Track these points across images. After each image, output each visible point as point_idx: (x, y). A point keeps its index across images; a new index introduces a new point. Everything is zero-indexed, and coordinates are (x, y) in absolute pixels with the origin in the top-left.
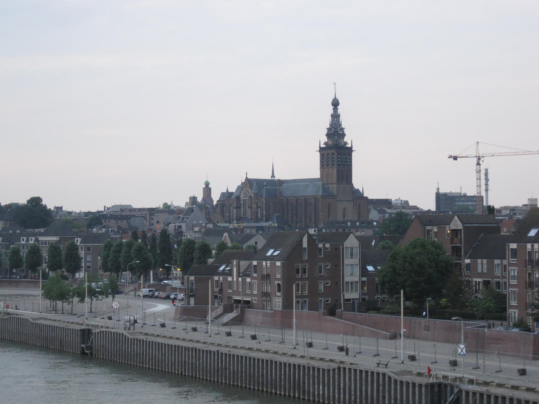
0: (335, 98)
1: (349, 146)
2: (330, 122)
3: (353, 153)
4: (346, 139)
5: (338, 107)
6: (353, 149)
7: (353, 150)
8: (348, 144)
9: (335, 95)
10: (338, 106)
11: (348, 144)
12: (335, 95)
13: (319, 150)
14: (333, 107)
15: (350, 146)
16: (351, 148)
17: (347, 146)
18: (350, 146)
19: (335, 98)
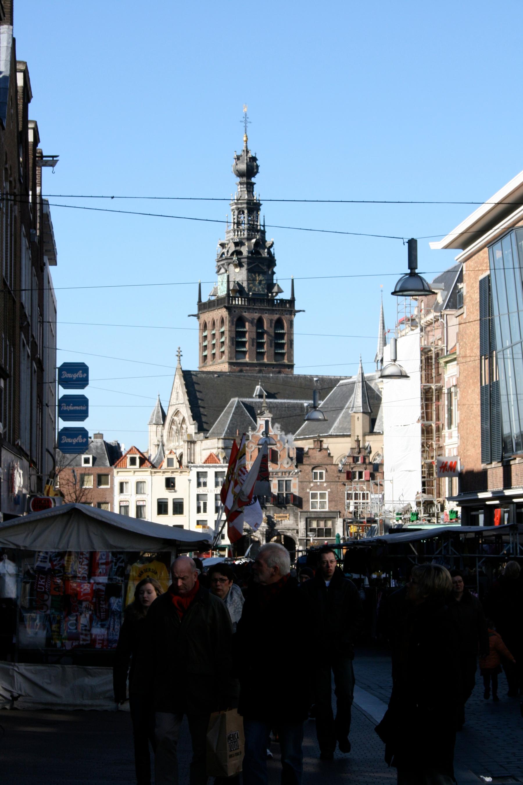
1: (286, 295)
3: (297, 319)
5: (253, 180)
6: (298, 306)
7: (297, 308)
10: (254, 176)
13: (196, 312)
14: (238, 180)
16: (292, 302)
17: (280, 296)
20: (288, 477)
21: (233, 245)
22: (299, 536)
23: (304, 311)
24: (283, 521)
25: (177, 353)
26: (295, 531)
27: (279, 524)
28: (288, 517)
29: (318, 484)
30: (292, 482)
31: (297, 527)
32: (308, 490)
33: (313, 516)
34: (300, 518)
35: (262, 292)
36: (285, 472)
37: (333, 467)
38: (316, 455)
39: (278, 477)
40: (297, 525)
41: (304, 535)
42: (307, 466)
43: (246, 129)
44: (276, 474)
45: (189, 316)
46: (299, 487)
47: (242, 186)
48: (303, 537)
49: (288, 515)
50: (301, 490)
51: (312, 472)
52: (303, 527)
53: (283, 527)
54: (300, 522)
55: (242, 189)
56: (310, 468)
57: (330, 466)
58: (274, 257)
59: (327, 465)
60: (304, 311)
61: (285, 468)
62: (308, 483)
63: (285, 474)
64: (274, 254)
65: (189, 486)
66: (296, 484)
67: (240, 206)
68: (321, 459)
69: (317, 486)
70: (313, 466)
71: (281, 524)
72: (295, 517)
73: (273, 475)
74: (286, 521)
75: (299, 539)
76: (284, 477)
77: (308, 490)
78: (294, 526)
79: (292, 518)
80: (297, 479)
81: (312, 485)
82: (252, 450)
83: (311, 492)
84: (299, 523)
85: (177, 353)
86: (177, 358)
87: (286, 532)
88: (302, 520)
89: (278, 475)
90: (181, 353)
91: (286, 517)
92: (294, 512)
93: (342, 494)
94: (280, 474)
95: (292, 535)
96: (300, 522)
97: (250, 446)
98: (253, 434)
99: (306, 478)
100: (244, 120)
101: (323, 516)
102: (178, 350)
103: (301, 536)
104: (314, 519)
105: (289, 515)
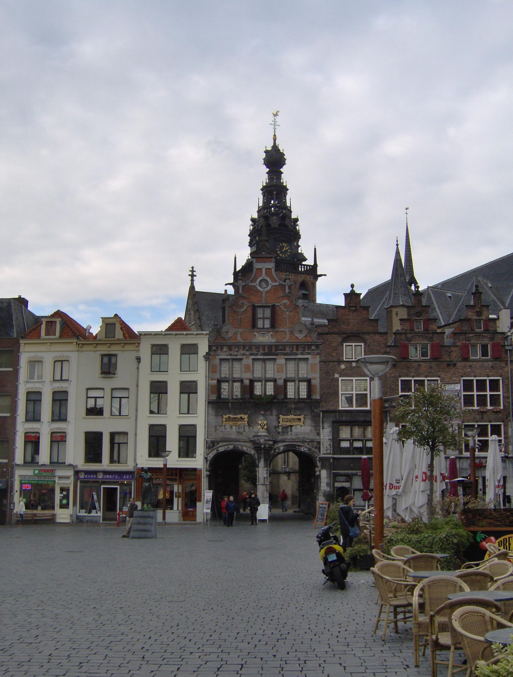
0: (275, 147)
1: (310, 262)
2: (259, 207)
4: (300, 249)
5: (281, 170)
7: (318, 273)
8: (305, 260)
9: (275, 140)
10: (281, 167)
11: (305, 260)
12: (275, 140)
13: (232, 281)
15: (312, 263)
16: (315, 267)
17: (304, 263)
18: (312, 263)
19: (275, 147)
20: (302, 354)
21: (263, 219)
22: (322, 452)
23: (325, 275)
24: (294, 428)
25: (191, 273)
26: (315, 444)
27: (288, 432)
28: (302, 420)
29: (354, 364)
30: (311, 361)
31: (318, 437)
32: (336, 376)
33: (344, 419)
34: (323, 423)
35: (288, 259)
36: (297, 346)
37: (377, 337)
38: (349, 317)
39: (285, 354)
40: (319, 434)
41: (329, 451)
42: (333, 335)
43: (275, 130)
44: (281, 350)
45: (226, 285)
46: (321, 370)
47: (271, 174)
48: (327, 454)
49: (302, 417)
50: (324, 375)
51: (343, 345)
52: (327, 438)
53: (294, 437)
54: (323, 428)
55: (271, 177)
56: (340, 339)
57: (373, 335)
58: (299, 232)
59: (368, 333)
60: (325, 275)
61: (297, 338)
62: (336, 364)
63: (297, 350)
64: (299, 230)
65: (138, 368)
66: (316, 364)
67: (269, 189)
68: (358, 324)
69: (352, 368)
70: (344, 336)
71: (290, 433)
72: (314, 421)
73: (276, 350)
74: (299, 427)
75: (321, 459)
76: (297, 354)
77: (336, 376)
78: (313, 436)
79: (309, 422)
80: (318, 356)
81: (343, 366)
82: (243, 310)
83: (340, 379)
84: (321, 429)
85: (191, 273)
86: (190, 278)
87: (299, 446)
88: (326, 425)
89: (285, 350)
90: (195, 274)
91: (299, 420)
92: (312, 411)
93: (393, 381)
94: (288, 350)
95: (310, 450)
96: (323, 428)
97: (240, 303)
98: (244, 284)
99: (333, 356)
100: (273, 123)
101: (362, 419)
102: (191, 269)
103: (325, 452)
104: (346, 423)
105: (304, 418)
